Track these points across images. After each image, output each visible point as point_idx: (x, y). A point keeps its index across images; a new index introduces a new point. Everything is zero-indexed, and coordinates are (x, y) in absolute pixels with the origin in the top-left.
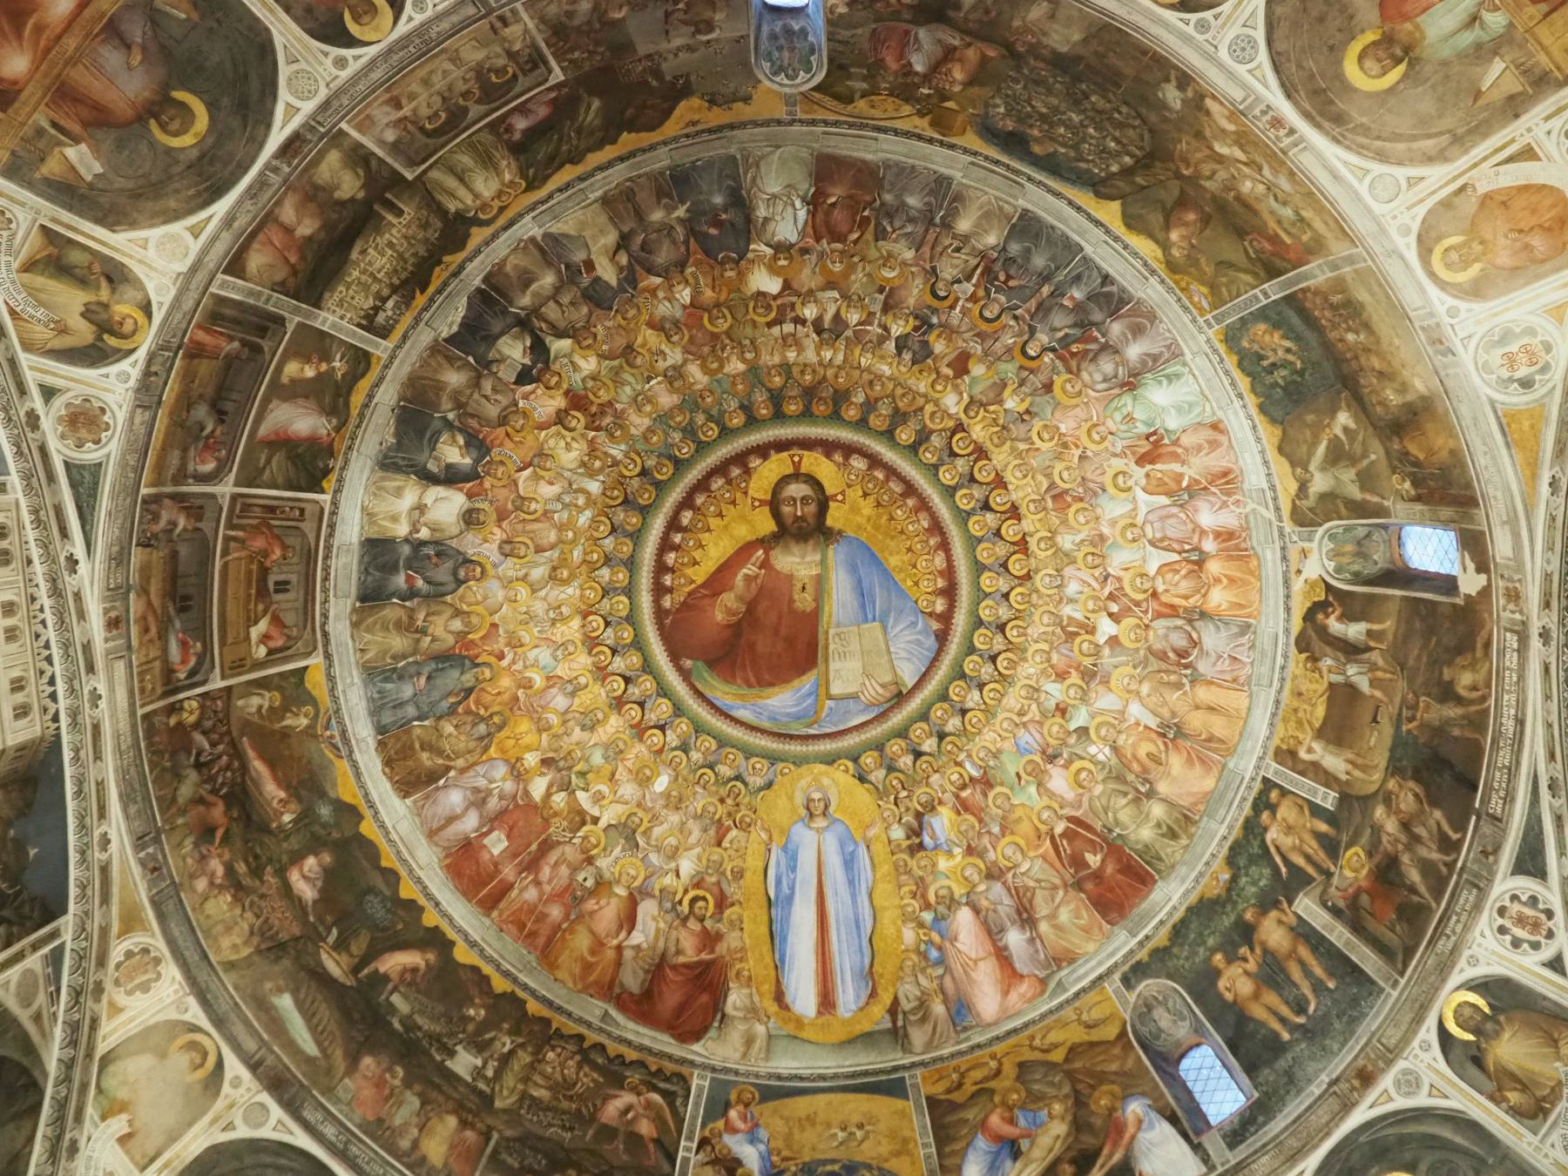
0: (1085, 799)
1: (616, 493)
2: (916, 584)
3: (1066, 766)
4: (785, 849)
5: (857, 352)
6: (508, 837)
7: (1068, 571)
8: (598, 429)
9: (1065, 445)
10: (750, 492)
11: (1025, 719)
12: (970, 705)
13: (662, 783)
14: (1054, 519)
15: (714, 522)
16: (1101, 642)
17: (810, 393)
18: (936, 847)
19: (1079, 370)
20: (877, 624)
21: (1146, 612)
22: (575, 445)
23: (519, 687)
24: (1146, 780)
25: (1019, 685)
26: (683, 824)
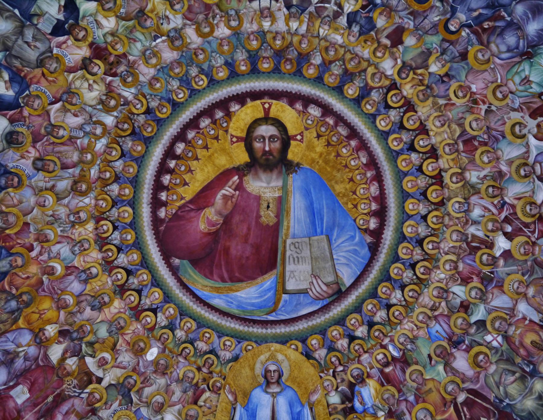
0: (482, 376)
1: (126, 126)
2: (355, 206)
3: (467, 351)
4: (246, 407)
5: (317, 23)
6: (30, 391)
7: (474, 199)
8: (115, 75)
9: (475, 102)
10: (230, 130)
11: (436, 313)
12: (394, 301)
13: (152, 354)
14: (464, 158)
15: (201, 153)
16: (498, 254)
17: (279, 54)
18: (365, 411)
19: (489, 43)
20: (324, 237)
21: (533, 232)
22: (95, 86)
23: (44, 274)
24: (531, 363)
25: (433, 286)
26: (168, 386)
